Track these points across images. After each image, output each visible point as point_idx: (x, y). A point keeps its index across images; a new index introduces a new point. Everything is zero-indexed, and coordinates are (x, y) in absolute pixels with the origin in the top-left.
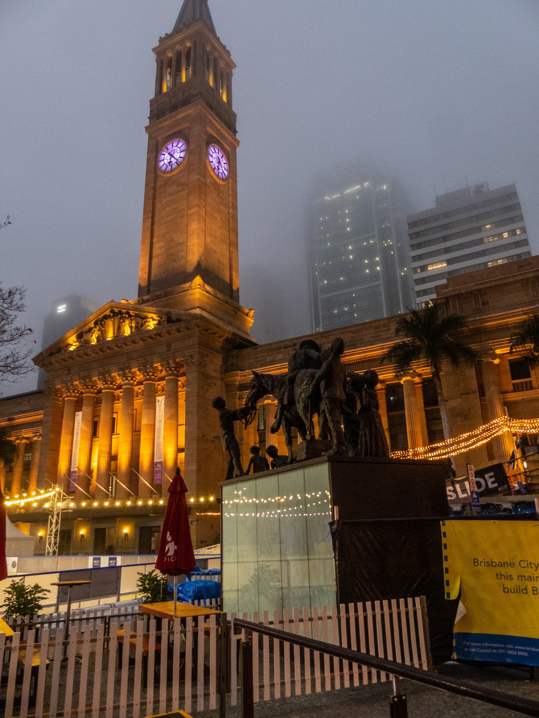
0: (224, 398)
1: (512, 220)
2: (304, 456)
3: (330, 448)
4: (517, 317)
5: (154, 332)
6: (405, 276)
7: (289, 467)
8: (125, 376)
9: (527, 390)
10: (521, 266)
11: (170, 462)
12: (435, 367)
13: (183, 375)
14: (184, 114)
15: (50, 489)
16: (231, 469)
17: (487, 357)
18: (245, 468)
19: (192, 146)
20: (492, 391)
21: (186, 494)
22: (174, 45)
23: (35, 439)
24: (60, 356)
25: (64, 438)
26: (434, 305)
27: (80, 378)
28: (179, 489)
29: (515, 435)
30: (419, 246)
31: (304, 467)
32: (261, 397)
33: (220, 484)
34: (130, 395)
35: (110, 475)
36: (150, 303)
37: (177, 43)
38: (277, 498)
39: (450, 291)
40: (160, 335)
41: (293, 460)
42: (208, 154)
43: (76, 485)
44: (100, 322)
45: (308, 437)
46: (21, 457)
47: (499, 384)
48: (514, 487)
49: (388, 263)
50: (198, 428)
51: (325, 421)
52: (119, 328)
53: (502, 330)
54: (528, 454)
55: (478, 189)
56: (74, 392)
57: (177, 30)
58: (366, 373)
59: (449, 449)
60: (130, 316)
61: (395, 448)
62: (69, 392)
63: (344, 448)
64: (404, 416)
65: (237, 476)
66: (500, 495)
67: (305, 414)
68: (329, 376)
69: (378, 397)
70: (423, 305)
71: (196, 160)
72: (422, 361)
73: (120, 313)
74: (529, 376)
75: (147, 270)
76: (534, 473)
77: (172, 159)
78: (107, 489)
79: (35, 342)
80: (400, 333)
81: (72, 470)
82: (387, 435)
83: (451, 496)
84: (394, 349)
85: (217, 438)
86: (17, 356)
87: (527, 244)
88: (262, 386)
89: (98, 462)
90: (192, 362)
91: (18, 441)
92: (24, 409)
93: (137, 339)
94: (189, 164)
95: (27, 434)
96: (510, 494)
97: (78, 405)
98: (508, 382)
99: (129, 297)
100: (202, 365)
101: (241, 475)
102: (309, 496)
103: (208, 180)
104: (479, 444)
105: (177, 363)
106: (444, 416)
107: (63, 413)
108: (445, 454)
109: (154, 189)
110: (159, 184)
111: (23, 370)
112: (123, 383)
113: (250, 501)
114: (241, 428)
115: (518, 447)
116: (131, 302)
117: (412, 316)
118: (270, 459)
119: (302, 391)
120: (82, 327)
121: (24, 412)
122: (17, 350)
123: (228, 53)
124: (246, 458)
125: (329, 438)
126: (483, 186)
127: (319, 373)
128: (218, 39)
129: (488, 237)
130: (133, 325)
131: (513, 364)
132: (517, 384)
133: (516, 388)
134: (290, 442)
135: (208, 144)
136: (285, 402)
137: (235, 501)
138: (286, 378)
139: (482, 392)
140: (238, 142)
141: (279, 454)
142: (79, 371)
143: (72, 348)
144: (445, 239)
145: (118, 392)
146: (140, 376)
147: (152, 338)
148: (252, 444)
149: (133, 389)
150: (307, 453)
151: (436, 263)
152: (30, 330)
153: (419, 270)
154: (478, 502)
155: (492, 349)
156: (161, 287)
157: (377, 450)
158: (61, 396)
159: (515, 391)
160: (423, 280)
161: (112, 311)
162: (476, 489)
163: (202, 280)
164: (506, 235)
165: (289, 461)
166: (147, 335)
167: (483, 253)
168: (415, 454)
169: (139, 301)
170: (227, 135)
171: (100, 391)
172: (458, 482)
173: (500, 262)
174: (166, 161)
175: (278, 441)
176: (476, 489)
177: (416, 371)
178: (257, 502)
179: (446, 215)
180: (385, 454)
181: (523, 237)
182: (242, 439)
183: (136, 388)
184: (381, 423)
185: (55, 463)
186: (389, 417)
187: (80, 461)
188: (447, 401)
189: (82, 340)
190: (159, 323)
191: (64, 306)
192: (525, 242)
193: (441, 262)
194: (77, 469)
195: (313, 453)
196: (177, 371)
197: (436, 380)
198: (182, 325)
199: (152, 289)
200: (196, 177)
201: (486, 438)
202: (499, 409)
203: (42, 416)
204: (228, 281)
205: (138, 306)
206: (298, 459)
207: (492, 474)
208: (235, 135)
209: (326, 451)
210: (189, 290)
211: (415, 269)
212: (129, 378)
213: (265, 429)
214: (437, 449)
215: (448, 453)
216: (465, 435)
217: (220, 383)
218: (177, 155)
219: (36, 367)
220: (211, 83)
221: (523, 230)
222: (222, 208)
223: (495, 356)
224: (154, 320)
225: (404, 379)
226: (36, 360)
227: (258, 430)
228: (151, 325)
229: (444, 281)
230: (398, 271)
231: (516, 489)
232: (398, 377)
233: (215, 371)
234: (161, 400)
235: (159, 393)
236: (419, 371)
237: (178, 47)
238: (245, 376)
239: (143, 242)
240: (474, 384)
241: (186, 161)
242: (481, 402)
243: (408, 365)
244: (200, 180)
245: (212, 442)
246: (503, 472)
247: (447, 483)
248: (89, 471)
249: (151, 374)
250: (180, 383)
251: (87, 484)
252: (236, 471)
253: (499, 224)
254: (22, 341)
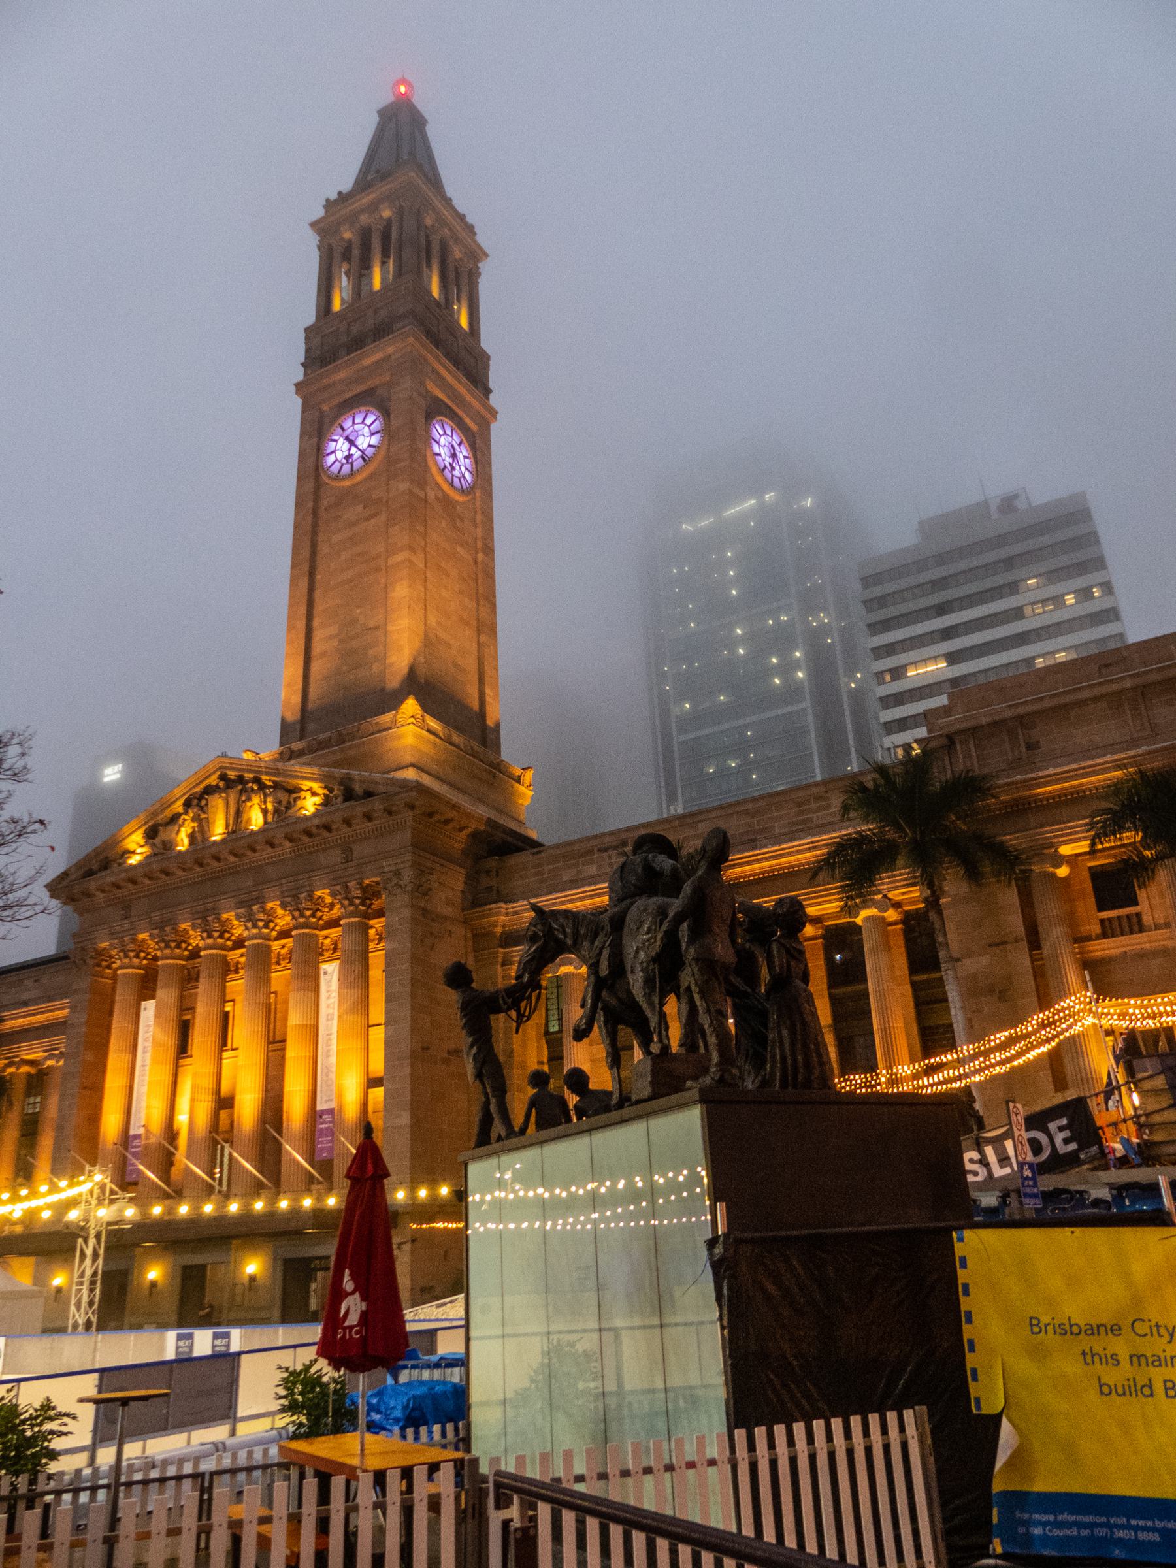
0: (471, 963)
1: (1082, 568)
2: (647, 1092)
3: (706, 1071)
4: (1103, 774)
5: (316, 822)
6: (860, 690)
7: (615, 1115)
8: (251, 919)
9: (1132, 933)
10: (1106, 666)
11: (351, 1110)
12: (931, 885)
13: (380, 914)
14: (378, 356)
15: (82, 1178)
16: (486, 1122)
17: (1043, 862)
18: (518, 1122)
19: (396, 422)
20: (1055, 936)
21: (385, 1181)
22: (355, 215)
23: (50, 1063)
24: (108, 878)
25: (115, 1061)
26: (924, 752)
27: (154, 925)
28: (370, 1169)
29: (1109, 1032)
30: (885, 625)
31: (647, 1115)
32: (552, 960)
33: (461, 1158)
34: (262, 961)
35: (217, 1143)
36: (305, 759)
37: (363, 211)
38: (590, 1187)
39: (956, 721)
40: (327, 827)
41: (624, 1100)
42: (429, 439)
43: (141, 1167)
44: (197, 801)
45: (655, 1048)
46: (17, 1106)
47: (1071, 921)
48: (1114, 1150)
49: (821, 664)
50: (414, 1031)
51: (693, 1012)
52: (238, 813)
53: (1073, 801)
54: (1141, 1075)
55: (1008, 504)
56: (137, 956)
57: (363, 183)
58: (780, 903)
59: (971, 1067)
60: (262, 787)
61: (847, 1068)
62: (126, 956)
63: (735, 1071)
64: (865, 995)
65: (500, 1139)
66: (1085, 1167)
67: (648, 997)
68: (699, 913)
69: (808, 955)
70: (900, 752)
71: (404, 451)
72: (902, 873)
73: (241, 780)
74: (1134, 902)
75: (300, 686)
76: (1157, 1118)
77: (354, 450)
78: (211, 1175)
79: (53, 849)
80: (852, 814)
81: (132, 1132)
82: (829, 1038)
83: (976, 1174)
84: (840, 849)
85: (456, 1052)
86: (11, 880)
87: (1117, 618)
88: (551, 937)
89: (191, 1113)
90: (397, 885)
91: (11, 1070)
92: (26, 996)
93: (279, 837)
94: (390, 461)
95: (32, 1052)
96: (1106, 1167)
97: (146, 987)
98: (1091, 917)
99: (260, 746)
100: (421, 891)
101: (508, 1137)
102: (661, 1181)
103: (431, 495)
104: (1031, 1055)
105: (365, 889)
106: (952, 992)
107: (112, 1003)
108: (960, 1078)
109: (315, 513)
111: (24, 912)
112: (246, 934)
113: (531, 1194)
114: (507, 1031)
115: (1117, 1059)
116: (266, 755)
117: (877, 776)
118: (572, 1099)
119: (640, 946)
120: (154, 814)
121: (25, 1004)
122: (11, 869)
123: (470, 229)
124: (520, 1099)
125: (702, 1050)
126: (1016, 496)
127: (676, 905)
128: (448, 201)
129: (1033, 604)
130: (270, 806)
131: (1098, 876)
132: (1110, 920)
133: (1108, 930)
134: (615, 1059)
135: (429, 417)
136: (604, 971)
137: (497, 1194)
138: (605, 917)
139: (1034, 940)
140: (493, 413)
141: (592, 1086)
142: (148, 910)
143: (134, 860)
144: (942, 610)
145: (235, 955)
146: (284, 919)
147: (309, 834)
148: (533, 1066)
149: (269, 947)
150: (652, 1083)
151: (925, 661)
152: (42, 822)
153: (888, 678)
154: (1035, 1185)
155: (1051, 845)
156: (329, 725)
157: (807, 1075)
158: (109, 967)
159: (1104, 935)
160: (898, 699)
161: (223, 777)
162: (1030, 1158)
163: (418, 707)
164: (1070, 599)
165: (614, 1101)
166: (300, 827)
167: (1022, 639)
168: (894, 1081)
169: (281, 754)
170: (469, 398)
171: (195, 954)
172: (990, 1141)
173: (1061, 657)
174: (340, 455)
175: (587, 1056)
176: (1030, 1158)
177: (890, 895)
178: (547, 1195)
179: (940, 559)
180: (826, 1082)
181: (1107, 604)
182: (510, 1054)
183: (276, 945)
184: (814, 1014)
185: (94, 1119)
186: (835, 1001)
187: (149, 1113)
188: (958, 960)
189: (157, 841)
190: (327, 802)
191: (119, 767)
192: (1112, 614)
193: (935, 658)
194: (142, 1131)
195: (667, 1084)
196: (366, 904)
197: (933, 915)
198: (376, 805)
199: (311, 726)
200: (403, 486)
201: (1048, 1041)
202: (1072, 976)
203: (65, 1012)
204: (475, 706)
205: (280, 766)
206: (634, 1098)
207: (1064, 1121)
208: (488, 399)
209: (695, 1078)
210: (390, 728)
211: (879, 675)
212: (261, 924)
213: (560, 1031)
214: (940, 1067)
215: (966, 1076)
216: (1002, 1036)
217: (459, 931)
218: (363, 442)
219: (55, 902)
220: (435, 291)
221: (1107, 588)
222: (459, 549)
223: (1059, 860)
224: (314, 794)
225: (864, 913)
226: (56, 888)
227: (547, 1033)
228: (309, 805)
229: (942, 700)
230: (844, 679)
231: (1118, 1155)
232: (850, 909)
233: (449, 903)
234: (331, 972)
235: (327, 954)
236: (894, 895)
237: (364, 219)
238: (515, 914)
239: (291, 628)
240: (1015, 923)
241: (383, 452)
242: (1032, 962)
243: (872, 883)
244: (411, 492)
245: (445, 1061)
246: (1089, 1118)
247: (964, 1144)
248: (171, 1134)
249: (308, 913)
250: (372, 932)
251: (165, 1161)
252: (498, 1128)
253: (1052, 576)
254: (24, 847)
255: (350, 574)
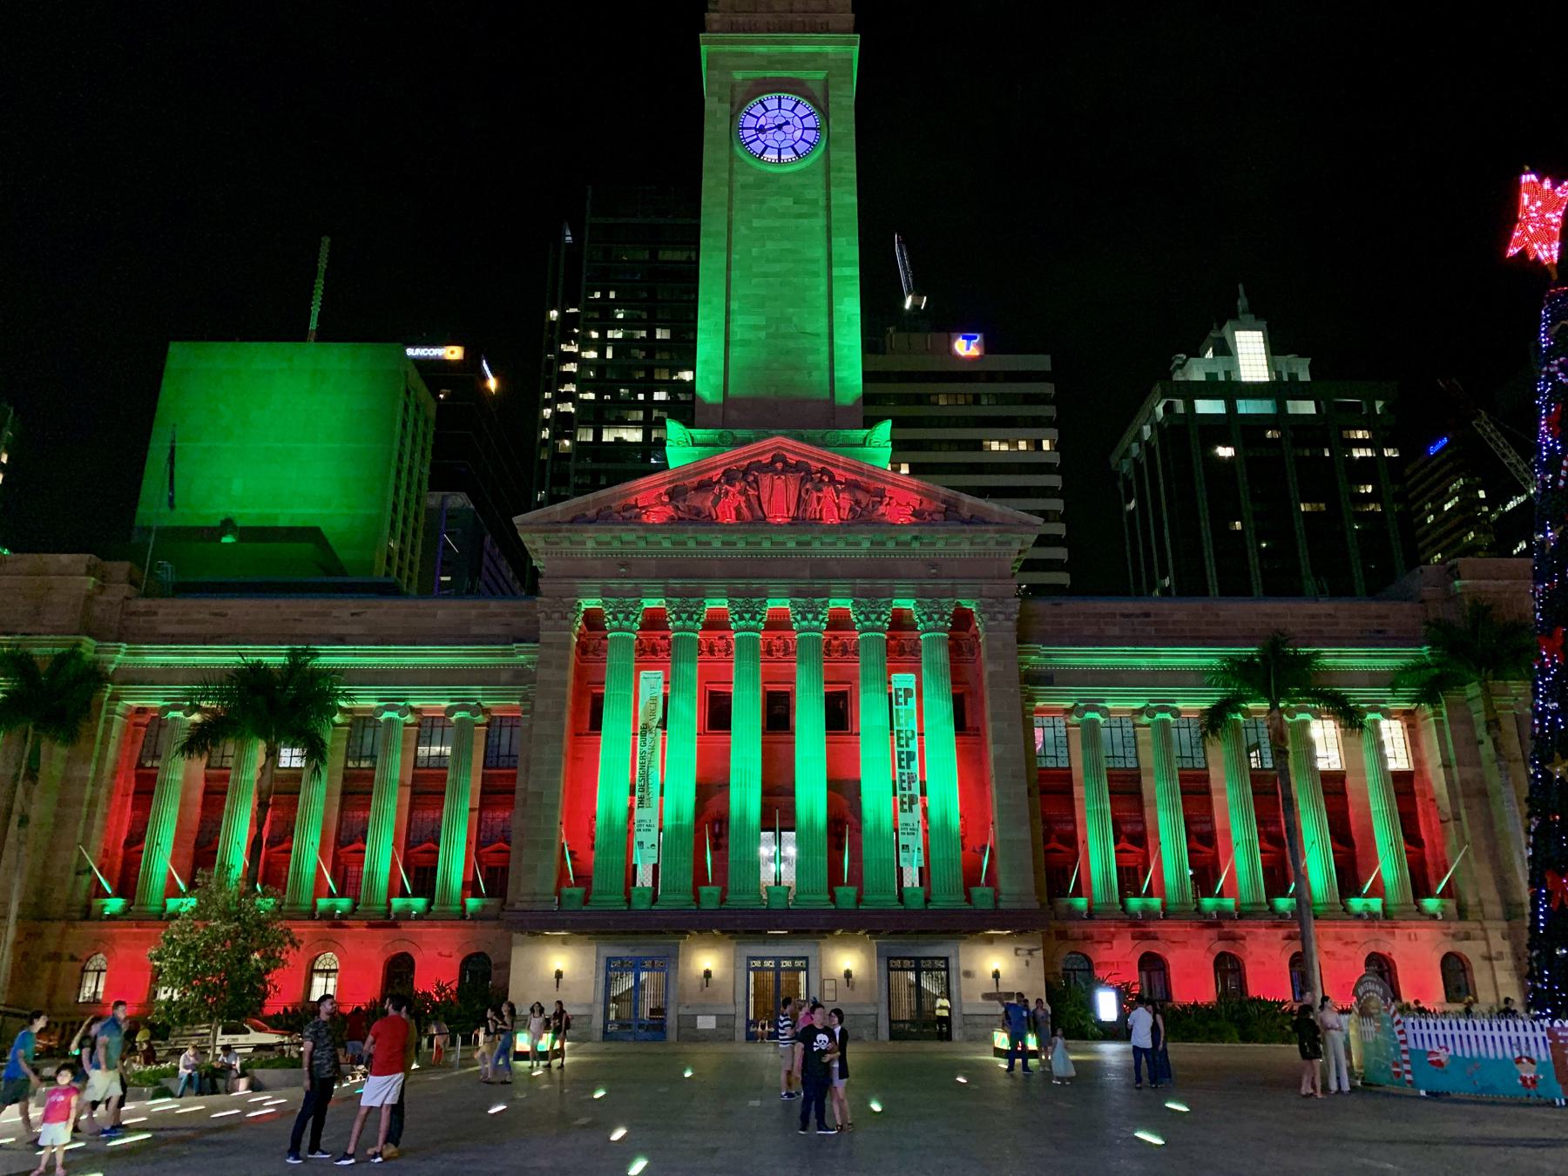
110: (740, 179)
210: (863, 445)
255: (777, 267)
